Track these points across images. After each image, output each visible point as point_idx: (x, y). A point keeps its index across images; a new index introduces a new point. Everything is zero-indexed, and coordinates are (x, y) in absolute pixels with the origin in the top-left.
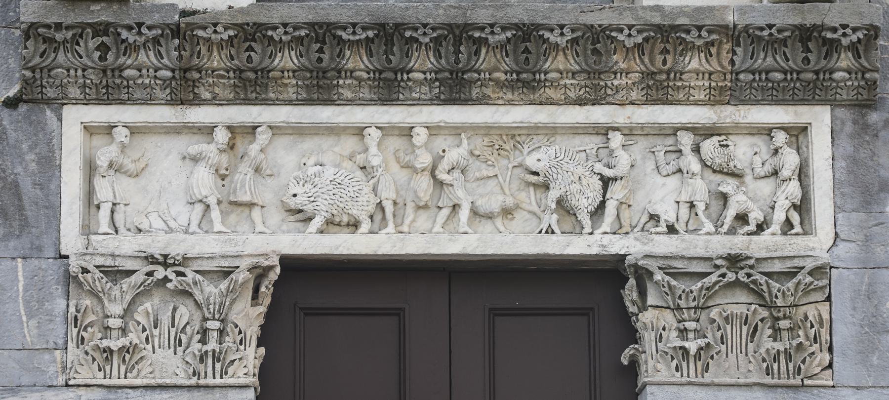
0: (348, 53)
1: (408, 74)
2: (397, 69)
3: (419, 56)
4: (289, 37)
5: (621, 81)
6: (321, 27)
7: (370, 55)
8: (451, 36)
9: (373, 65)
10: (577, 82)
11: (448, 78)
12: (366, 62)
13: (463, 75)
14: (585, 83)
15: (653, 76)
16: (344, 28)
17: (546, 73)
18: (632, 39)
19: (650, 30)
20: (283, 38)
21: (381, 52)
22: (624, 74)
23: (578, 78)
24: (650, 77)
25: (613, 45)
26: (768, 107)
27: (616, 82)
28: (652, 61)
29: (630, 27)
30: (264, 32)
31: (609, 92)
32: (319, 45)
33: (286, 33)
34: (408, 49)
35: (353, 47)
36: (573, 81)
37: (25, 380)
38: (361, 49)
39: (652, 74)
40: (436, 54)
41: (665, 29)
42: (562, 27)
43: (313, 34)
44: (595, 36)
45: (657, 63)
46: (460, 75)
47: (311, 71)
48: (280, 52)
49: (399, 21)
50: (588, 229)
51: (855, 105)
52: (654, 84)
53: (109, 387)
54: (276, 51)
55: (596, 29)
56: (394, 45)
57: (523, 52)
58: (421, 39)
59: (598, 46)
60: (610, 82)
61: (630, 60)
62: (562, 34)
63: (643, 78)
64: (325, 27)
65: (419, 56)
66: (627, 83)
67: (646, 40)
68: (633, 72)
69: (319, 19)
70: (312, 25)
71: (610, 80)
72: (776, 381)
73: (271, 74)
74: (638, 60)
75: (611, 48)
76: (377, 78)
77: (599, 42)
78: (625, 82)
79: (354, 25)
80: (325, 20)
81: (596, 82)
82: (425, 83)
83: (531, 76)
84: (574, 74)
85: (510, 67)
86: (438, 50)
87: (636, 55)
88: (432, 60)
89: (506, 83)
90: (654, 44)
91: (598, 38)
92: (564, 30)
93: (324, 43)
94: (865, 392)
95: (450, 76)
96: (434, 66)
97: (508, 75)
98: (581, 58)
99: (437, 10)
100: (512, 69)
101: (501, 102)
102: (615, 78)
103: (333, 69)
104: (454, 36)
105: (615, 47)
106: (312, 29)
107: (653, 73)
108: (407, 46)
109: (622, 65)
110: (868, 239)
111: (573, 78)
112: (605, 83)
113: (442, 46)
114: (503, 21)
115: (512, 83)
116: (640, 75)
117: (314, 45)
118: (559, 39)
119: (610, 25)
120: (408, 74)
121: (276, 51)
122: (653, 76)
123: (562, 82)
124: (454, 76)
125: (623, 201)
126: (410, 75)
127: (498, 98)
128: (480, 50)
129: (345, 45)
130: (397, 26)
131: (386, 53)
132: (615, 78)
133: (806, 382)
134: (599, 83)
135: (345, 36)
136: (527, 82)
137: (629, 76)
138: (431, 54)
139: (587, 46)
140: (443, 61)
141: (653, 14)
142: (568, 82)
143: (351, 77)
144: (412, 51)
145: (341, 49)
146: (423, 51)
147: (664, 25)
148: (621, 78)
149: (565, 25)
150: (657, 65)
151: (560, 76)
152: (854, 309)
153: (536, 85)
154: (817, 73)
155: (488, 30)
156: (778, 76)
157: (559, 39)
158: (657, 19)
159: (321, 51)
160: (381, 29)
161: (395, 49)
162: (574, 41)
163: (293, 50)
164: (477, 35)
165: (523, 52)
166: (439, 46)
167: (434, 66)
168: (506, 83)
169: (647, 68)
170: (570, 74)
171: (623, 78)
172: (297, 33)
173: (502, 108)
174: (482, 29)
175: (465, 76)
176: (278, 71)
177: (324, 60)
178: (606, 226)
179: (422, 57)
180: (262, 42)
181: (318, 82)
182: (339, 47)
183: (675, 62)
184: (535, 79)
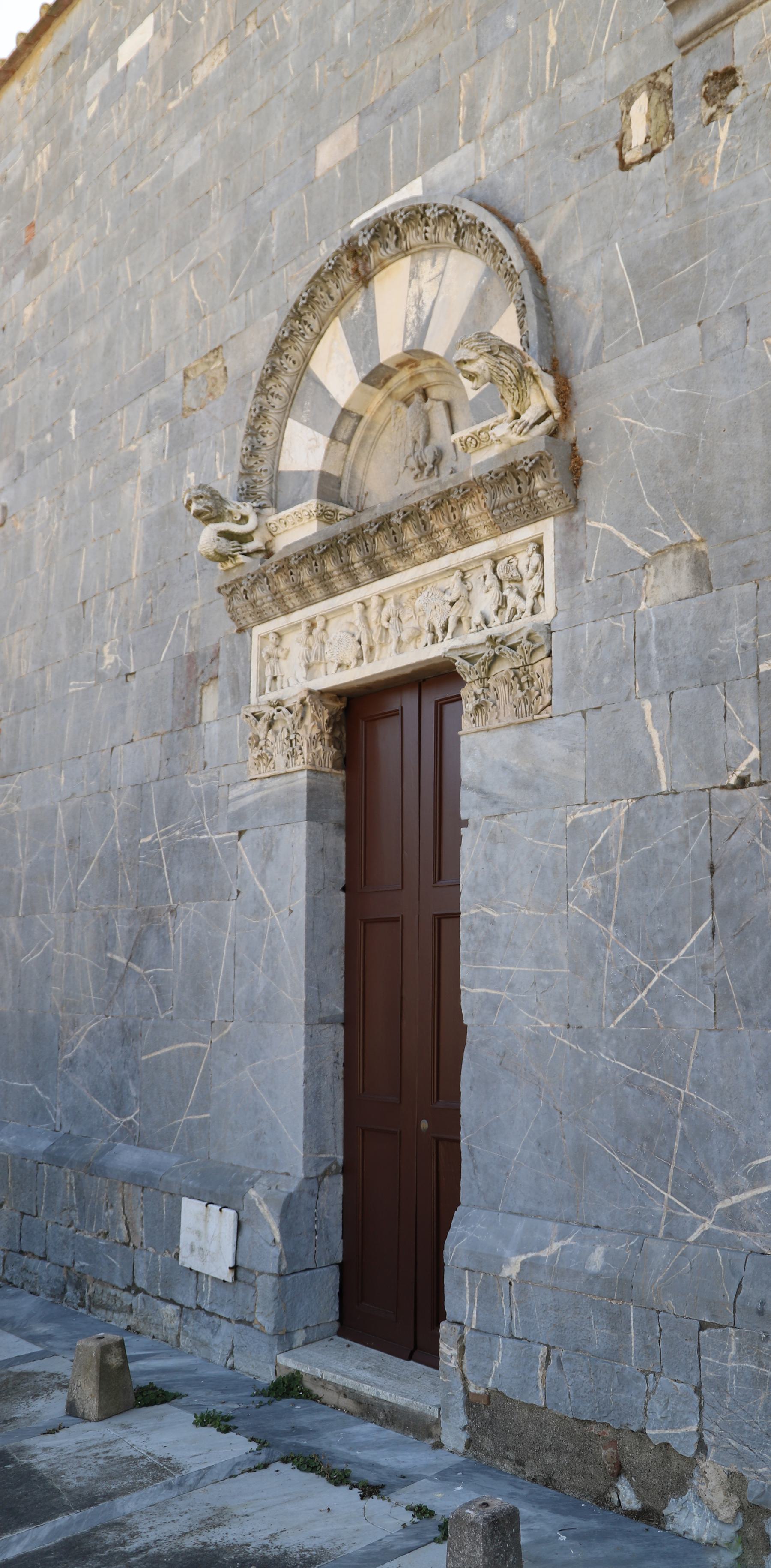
26: (522, 529)
31: (443, 546)
37: (238, 780)
50: (440, 640)
51: (567, 511)
53: (262, 779)
72: (521, 720)
94: (567, 717)
101: (401, 569)
109: (437, 526)
110: (572, 606)
125: (459, 615)
127: (399, 567)
133: (536, 717)
152: (564, 659)
154: (529, 495)
156: (510, 506)
173: (404, 573)
178: (449, 635)
183: (460, 515)
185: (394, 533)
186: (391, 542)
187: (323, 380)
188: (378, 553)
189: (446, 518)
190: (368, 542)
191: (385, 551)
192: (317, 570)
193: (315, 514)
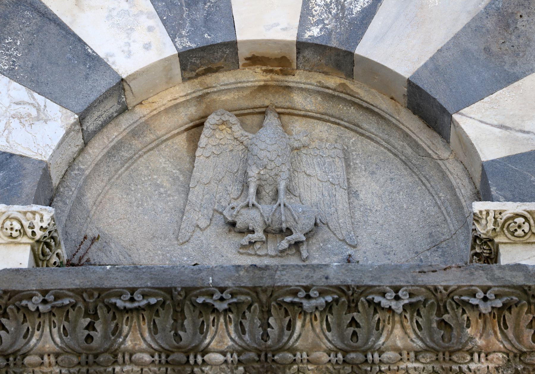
0: (126, 329)
1: (203, 356)
2: (189, 347)
3: (216, 332)
4: (49, 307)
5: (479, 365)
6: (91, 295)
7: (154, 330)
8: (256, 304)
9: (157, 343)
10: (421, 366)
11: (254, 361)
12: (149, 339)
13: (273, 356)
14: (433, 367)
15: (522, 358)
16: (119, 295)
17: (381, 352)
18: (489, 303)
19: (513, 294)
20: (41, 307)
21: (168, 326)
22: (483, 355)
23: (423, 360)
24: (518, 360)
25: (465, 316)
27: (473, 366)
28: (518, 337)
29: (486, 290)
30: (17, 303)
32: (89, 320)
33: (44, 302)
34: (203, 322)
35: (132, 321)
36: (416, 365)
38: (142, 324)
39: (520, 356)
40: (238, 329)
41: (530, 293)
42: (397, 289)
43: (80, 305)
44: (441, 305)
45: (525, 338)
46: (269, 355)
47: (79, 354)
48: (38, 330)
49: (190, 284)
52: (524, 369)
54: (33, 329)
55: (441, 292)
56: (185, 318)
57: (350, 325)
58: (218, 305)
59: (446, 317)
60: (466, 366)
61: (488, 335)
62: (397, 298)
63: (509, 361)
64: (96, 294)
65: (216, 332)
66: (488, 367)
67: (507, 306)
68: (494, 352)
69: (88, 285)
70: (79, 292)
71: (466, 363)
73: (27, 360)
74: (499, 335)
75: (463, 320)
76: (163, 361)
77: (447, 312)
78: (485, 365)
79: (133, 291)
80: (96, 284)
81: (446, 366)
82: (226, 369)
83: (361, 357)
84: (417, 353)
85: (333, 344)
86: (241, 323)
87: (497, 329)
88: (233, 335)
89: (329, 366)
90: (519, 314)
91: (445, 307)
92: (400, 294)
93: (95, 316)
95: (257, 358)
96: (236, 343)
97: (332, 355)
98: (425, 332)
99: (237, 271)
100: (336, 347)
102: (472, 360)
103: (106, 351)
104: (261, 305)
105: (468, 318)
106: (80, 299)
107: (523, 353)
108: (201, 319)
109: (480, 342)
111: (417, 360)
112: (460, 367)
113: (246, 319)
114: (322, 283)
115: (337, 367)
116: (505, 356)
117: (82, 320)
118: (393, 304)
119: (459, 287)
120: (203, 356)
121: (33, 329)
122: (522, 358)
123: (403, 365)
124: (263, 358)
126: (206, 358)
128: (295, 324)
129: (123, 320)
130: (188, 291)
131: (175, 328)
132: (472, 360)
134: (451, 368)
135: (120, 303)
136: (357, 365)
137: (490, 357)
138: (231, 328)
139: (432, 318)
140: (247, 337)
141: (514, 273)
142: (410, 365)
143: (131, 361)
144: (208, 326)
145: (117, 325)
146: (221, 325)
147: (530, 287)
148: (479, 361)
149: (401, 287)
150: (525, 341)
151: (400, 357)
153: (369, 369)
155: (302, 294)
157: (393, 304)
158: (519, 280)
159: (91, 327)
160: (168, 297)
161: (186, 323)
162: (412, 307)
163: (55, 327)
164: (288, 299)
165: (350, 325)
166: (242, 319)
167: (236, 343)
168: (329, 366)
169: (513, 346)
170: (412, 354)
171: (483, 360)
172: (59, 303)
174: (295, 293)
175: (276, 357)
176: (36, 354)
177: (94, 338)
179: (220, 332)
180: (16, 319)
181: (88, 370)
182: (115, 322)
184: (366, 361)
185: (354, 322)
186: (342, 338)
187: (66, 19)
188: (293, 350)
189: (510, 334)
190: (271, 321)
191: (315, 347)
192: (89, 338)
193: (39, 234)
